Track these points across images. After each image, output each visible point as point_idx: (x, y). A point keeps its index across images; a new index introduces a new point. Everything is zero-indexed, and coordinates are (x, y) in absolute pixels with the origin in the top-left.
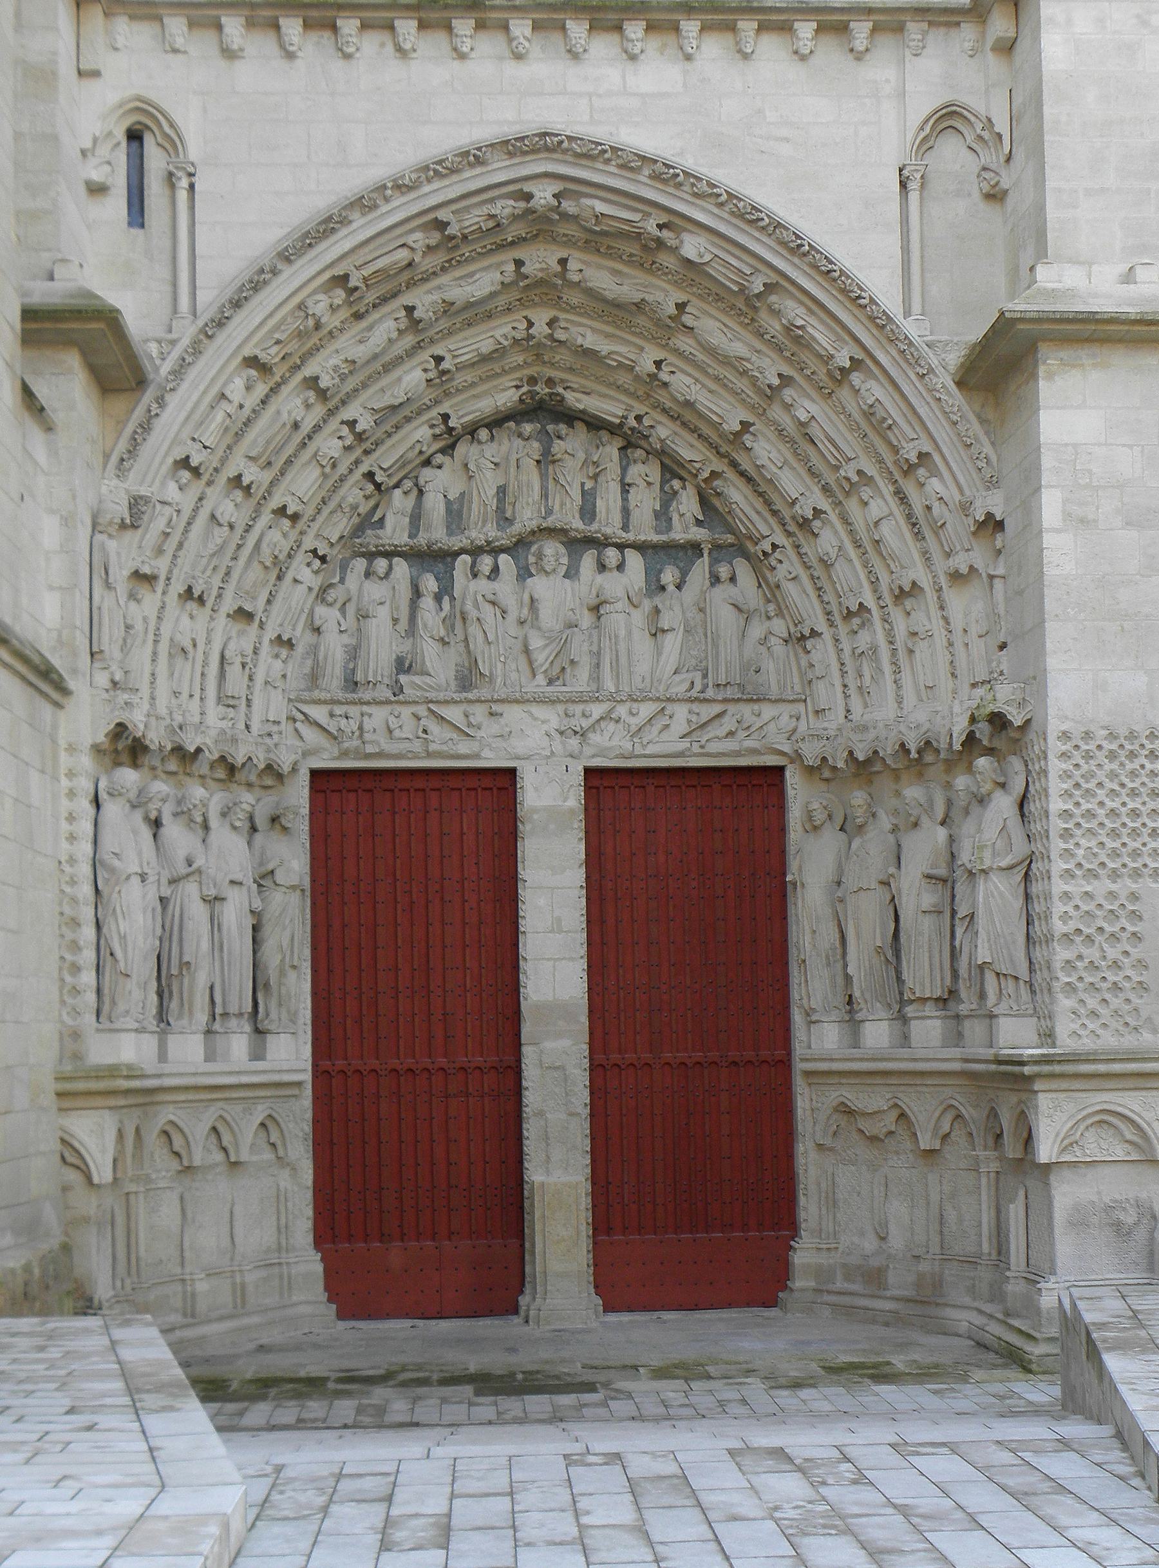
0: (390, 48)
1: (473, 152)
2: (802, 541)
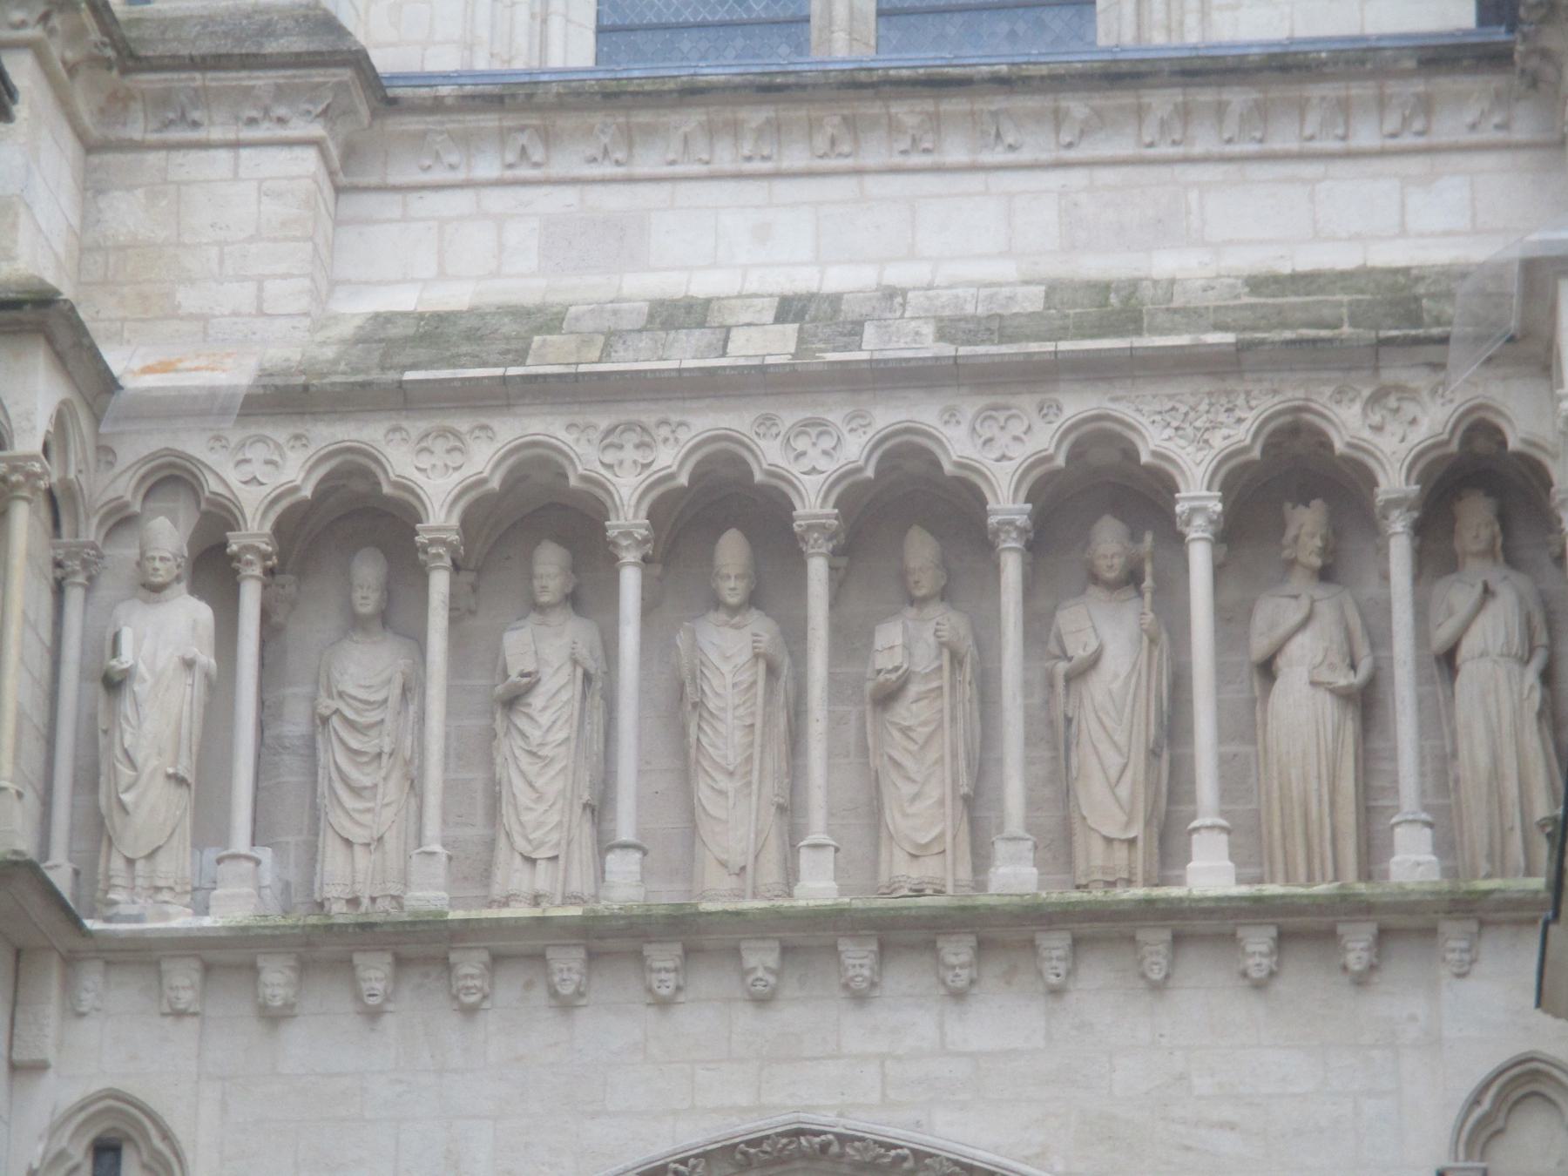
0: (540, 994)
1: (673, 1166)
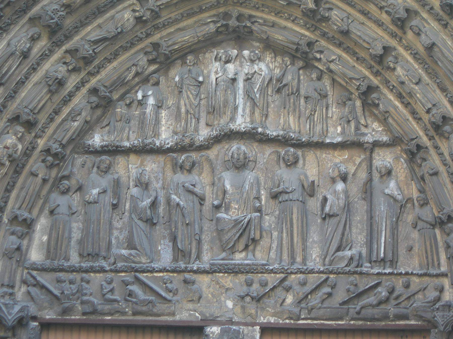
2: (440, 144)
